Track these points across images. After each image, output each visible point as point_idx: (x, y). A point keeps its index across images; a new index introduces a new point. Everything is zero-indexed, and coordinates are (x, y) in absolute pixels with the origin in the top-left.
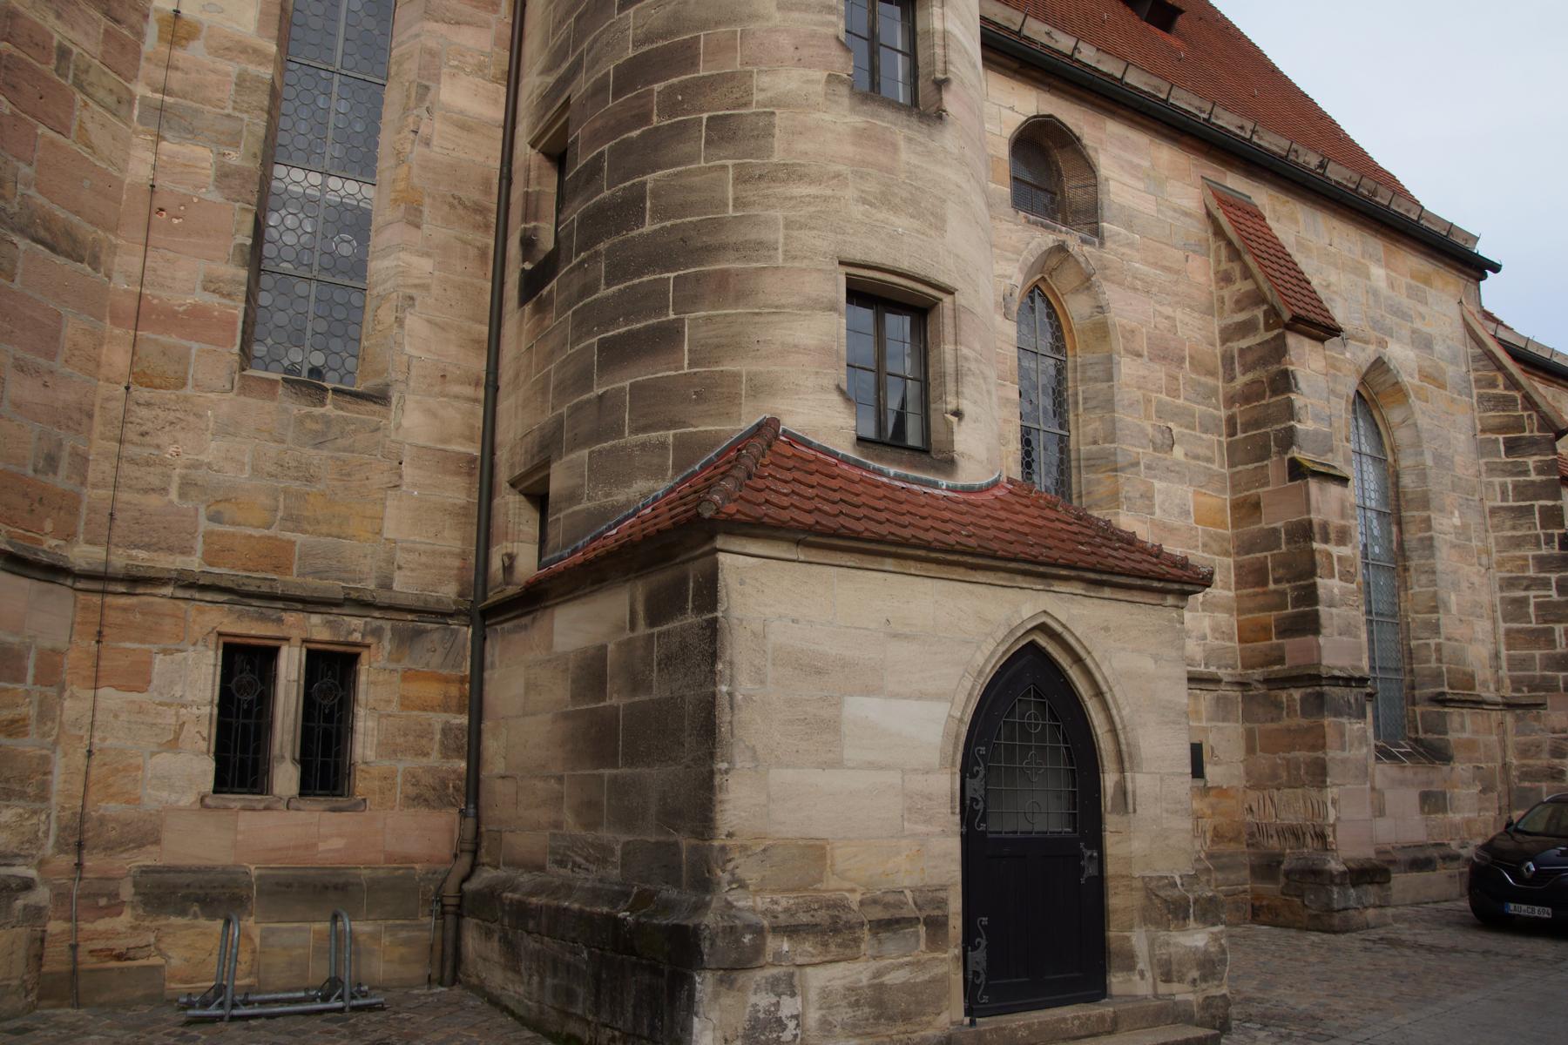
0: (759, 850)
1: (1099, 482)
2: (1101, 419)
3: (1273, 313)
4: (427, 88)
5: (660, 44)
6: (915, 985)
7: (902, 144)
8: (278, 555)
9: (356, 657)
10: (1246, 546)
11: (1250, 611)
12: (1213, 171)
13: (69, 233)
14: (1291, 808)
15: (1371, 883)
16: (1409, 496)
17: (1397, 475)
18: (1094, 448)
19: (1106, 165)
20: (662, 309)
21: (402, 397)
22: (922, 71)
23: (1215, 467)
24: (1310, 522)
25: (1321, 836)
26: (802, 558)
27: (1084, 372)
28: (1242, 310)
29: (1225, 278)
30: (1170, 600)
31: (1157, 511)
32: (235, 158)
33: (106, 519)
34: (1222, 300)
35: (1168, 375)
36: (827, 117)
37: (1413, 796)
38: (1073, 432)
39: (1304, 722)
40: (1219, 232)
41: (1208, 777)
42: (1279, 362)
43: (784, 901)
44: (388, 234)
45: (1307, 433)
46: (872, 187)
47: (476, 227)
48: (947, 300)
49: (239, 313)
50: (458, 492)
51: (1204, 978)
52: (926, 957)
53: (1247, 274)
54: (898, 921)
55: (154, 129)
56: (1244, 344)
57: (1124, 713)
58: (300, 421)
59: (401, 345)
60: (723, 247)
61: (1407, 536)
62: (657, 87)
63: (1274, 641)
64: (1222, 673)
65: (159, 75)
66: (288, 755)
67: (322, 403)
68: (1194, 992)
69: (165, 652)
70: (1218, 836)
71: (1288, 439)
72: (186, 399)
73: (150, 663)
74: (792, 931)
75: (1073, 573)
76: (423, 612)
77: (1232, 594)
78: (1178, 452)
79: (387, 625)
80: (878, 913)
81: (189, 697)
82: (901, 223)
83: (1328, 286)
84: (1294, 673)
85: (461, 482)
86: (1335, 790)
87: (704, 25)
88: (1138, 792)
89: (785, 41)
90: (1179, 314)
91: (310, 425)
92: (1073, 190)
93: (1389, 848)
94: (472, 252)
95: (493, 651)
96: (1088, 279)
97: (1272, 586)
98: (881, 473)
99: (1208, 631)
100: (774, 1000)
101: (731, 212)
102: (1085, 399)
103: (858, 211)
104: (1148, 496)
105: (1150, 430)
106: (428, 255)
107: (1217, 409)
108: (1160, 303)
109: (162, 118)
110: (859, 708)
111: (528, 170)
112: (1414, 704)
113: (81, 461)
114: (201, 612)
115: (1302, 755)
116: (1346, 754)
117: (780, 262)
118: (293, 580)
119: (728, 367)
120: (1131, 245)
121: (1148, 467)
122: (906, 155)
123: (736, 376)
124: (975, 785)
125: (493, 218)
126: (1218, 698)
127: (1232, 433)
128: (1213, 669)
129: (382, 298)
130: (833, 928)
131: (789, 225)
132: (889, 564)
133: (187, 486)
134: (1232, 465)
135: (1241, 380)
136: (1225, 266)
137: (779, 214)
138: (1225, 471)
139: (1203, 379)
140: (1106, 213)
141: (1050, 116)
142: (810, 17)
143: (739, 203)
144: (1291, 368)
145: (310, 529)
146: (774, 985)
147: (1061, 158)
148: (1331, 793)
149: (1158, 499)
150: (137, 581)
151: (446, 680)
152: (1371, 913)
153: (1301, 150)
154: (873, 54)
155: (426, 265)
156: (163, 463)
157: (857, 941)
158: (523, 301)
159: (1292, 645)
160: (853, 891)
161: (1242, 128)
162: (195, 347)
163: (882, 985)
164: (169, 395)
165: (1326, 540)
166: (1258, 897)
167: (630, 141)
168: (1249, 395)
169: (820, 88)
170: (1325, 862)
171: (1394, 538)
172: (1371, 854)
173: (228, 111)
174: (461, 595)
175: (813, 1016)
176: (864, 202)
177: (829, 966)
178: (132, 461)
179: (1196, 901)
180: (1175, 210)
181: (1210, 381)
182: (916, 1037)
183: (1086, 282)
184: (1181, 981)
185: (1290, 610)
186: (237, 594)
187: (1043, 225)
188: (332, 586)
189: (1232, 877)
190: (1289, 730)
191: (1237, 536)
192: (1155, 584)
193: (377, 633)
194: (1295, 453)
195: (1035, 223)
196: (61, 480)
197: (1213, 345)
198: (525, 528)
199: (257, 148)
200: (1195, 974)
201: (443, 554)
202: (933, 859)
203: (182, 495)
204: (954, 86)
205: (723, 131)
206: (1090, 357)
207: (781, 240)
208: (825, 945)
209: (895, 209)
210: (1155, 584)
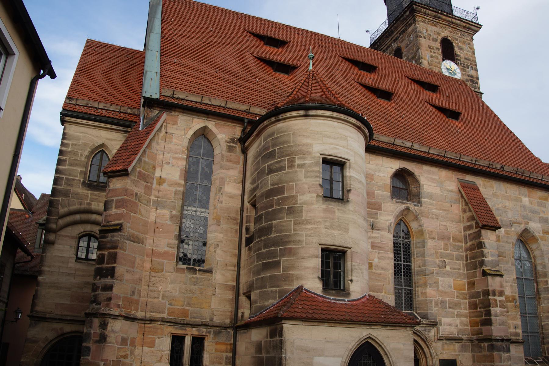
1: (421, 279)
3: (477, 223)
5: (276, 186)
7: (336, 211)
8: (185, 313)
9: (204, 338)
10: (472, 296)
11: (473, 317)
12: (461, 176)
13: (137, 238)
19: (423, 180)
20: (276, 257)
21: (216, 271)
22: (345, 187)
23: (461, 271)
24: (488, 290)
28: (469, 221)
29: (464, 211)
31: (440, 287)
32: (174, 212)
33: (145, 305)
34: (463, 218)
36: (316, 206)
39: (488, 353)
40: (462, 196)
42: (479, 239)
44: (212, 227)
45: (489, 261)
46: (328, 224)
47: (234, 224)
49: (176, 252)
50: (230, 295)
53: (470, 211)
55: (155, 207)
56: (470, 232)
58: (191, 279)
60: (290, 242)
62: (275, 198)
64: (464, 337)
65: (157, 193)
66: (187, 363)
67: (196, 274)
69: (158, 338)
71: (482, 263)
72: (163, 275)
73: (155, 341)
76: (221, 327)
77: (467, 311)
78: (448, 268)
79: (212, 330)
81: (164, 349)
82: (336, 232)
83: (505, 207)
85: (231, 292)
87: (286, 182)
89: (306, 186)
90: (448, 224)
91: (193, 280)
92: (413, 189)
94: (234, 231)
95: (239, 337)
97: (478, 310)
99: (458, 324)
101: (292, 232)
103: (324, 231)
104: (437, 283)
105: (438, 262)
106: (222, 233)
108: (442, 221)
109: (158, 204)
111: (247, 209)
113: (140, 291)
114: (167, 328)
116: (502, 364)
118: (189, 319)
120: (431, 204)
121: (437, 274)
122: (338, 214)
125: (239, 221)
126: (462, 345)
127: (467, 261)
128: (460, 336)
129: (211, 245)
131: (306, 236)
133: (164, 296)
134: (467, 271)
135: (469, 244)
136: (464, 207)
137: (304, 233)
138: (465, 272)
139: (457, 244)
140: (423, 195)
142: (312, 179)
143: (294, 230)
144: (483, 241)
147: (409, 179)
149: (440, 283)
150: (152, 320)
151: (227, 344)
153: (493, 164)
154: (331, 184)
155: (222, 236)
156: (158, 291)
158: (246, 246)
159: (484, 328)
161: (471, 160)
162: (165, 261)
164: (159, 274)
165: (494, 295)
167: (268, 212)
168: (471, 249)
169: (315, 199)
173: (173, 200)
174: (231, 322)
176: (326, 228)
178: (151, 291)
180: (447, 191)
181: (460, 244)
183: (416, 218)
185: (483, 318)
186: (175, 323)
188: (198, 321)
191: (469, 293)
193: (209, 332)
195: (399, 202)
196: (135, 297)
197: (461, 232)
198: (247, 305)
199: (179, 209)
201: (226, 312)
203: (162, 299)
204: (352, 191)
205: (291, 211)
206: (418, 240)
209: (334, 229)
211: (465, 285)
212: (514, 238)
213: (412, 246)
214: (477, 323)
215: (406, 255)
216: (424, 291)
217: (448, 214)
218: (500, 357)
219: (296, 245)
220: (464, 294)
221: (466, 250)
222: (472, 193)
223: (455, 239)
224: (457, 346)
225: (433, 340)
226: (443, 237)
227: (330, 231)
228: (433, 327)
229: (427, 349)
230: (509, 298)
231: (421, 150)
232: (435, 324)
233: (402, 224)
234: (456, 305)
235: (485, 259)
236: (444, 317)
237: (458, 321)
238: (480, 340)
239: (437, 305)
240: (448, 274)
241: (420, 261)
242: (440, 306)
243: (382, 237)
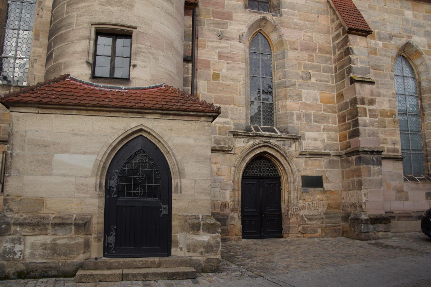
0: (18, 200)
1: (281, 92)
2: (281, 71)
3: (344, 29)
4: (41, 2)
6: (69, 244)
14: (350, 198)
15: (381, 223)
16: (424, 90)
17: (420, 83)
18: (279, 81)
23: (330, 84)
24: (356, 98)
25: (361, 207)
26: (40, 112)
27: (276, 57)
28: (337, 30)
29: (333, 21)
30: (203, 119)
31: (304, 100)
34: (332, 29)
35: (308, 55)
37: (423, 194)
38: (273, 77)
41: (325, 187)
43: (25, 216)
45: (357, 68)
48: (135, 31)
51: (207, 252)
52: (74, 236)
54: (63, 224)
56: (337, 41)
57: (177, 158)
59: (32, 72)
61: (424, 104)
63: (348, 140)
64: (332, 153)
68: (203, 257)
70: (329, 207)
71: (350, 70)
74: (21, 225)
75: (151, 111)
77: (337, 126)
78: (313, 80)
80: (58, 221)
82: (114, 9)
83: (384, 20)
84: (352, 151)
86: (366, 190)
88: (183, 186)
90: (314, 35)
93: (410, 212)
96: (275, 27)
98: (98, 86)
99: (326, 138)
100: (13, 245)
101: (65, 16)
102: (277, 66)
103: (98, 8)
104: (299, 95)
105: (301, 74)
108: (306, 32)
110: (59, 157)
112: (427, 162)
115: (356, 179)
116: (371, 178)
117: (74, 28)
119: (60, 61)
120: (294, 15)
121: (300, 85)
123: (61, 63)
124: (113, 183)
126: (330, 161)
128: (328, 151)
130: (39, 225)
132: (74, 112)
134: (336, 83)
135: (338, 53)
136: (332, 17)
139: (324, 55)
140: (283, 5)
143: (67, 13)
145: (6, 123)
146: (13, 241)
148: (363, 192)
149: (303, 96)
152: (380, 234)
155: (40, 50)
157: (46, 229)
159: (352, 140)
160: (53, 214)
163: (56, 244)
165: (363, 103)
166: (343, 228)
168: (339, 59)
170: (361, 215)
171: (419, 104)
172: (383, 213)
175: (28, 252)
176: (100, 4)
177: (36, 236)
179: (204, 224)
181: (328, 56)
182: (69, 261)
183: (275, 28)
184: (194, 252)
185: (351, 129)
187: (256, 12)
189: (334, 221)
190: (352, 170)
191: (338, 106)
192: (191, 113)
194: (352, 75)
195: (253, 12)
197: (329, 44)
200: (202, 250)
202: (92, 205)
206: (278, 52)
207: (75, 21)
208: (34, 229)
209: (111, 5)
210: (191, 113)
211: (333, 98)
212: (394, 52)
214: (346, 136)
216: (284, 104)
217: (314, 25)
218: (369, 171)
219: (67, 29)
220: (333, 107)
221: (335, 61)
223: (321, 50)
224: (324, 161)
225: (294, 155)
227: (106, 8)
228: (295, 142)
229: (288, 165)
230: (387, 112)
232: (296, 139)
233: (260, 37)
234: (324, 119)
235: (353, 66)
236: (308, 131)
237: (325, 135)
238: (349, 154)
239: (299, 118)
240: (313, 87)
241: (280, 73)
242: (303, 119)
243: (232, 47)
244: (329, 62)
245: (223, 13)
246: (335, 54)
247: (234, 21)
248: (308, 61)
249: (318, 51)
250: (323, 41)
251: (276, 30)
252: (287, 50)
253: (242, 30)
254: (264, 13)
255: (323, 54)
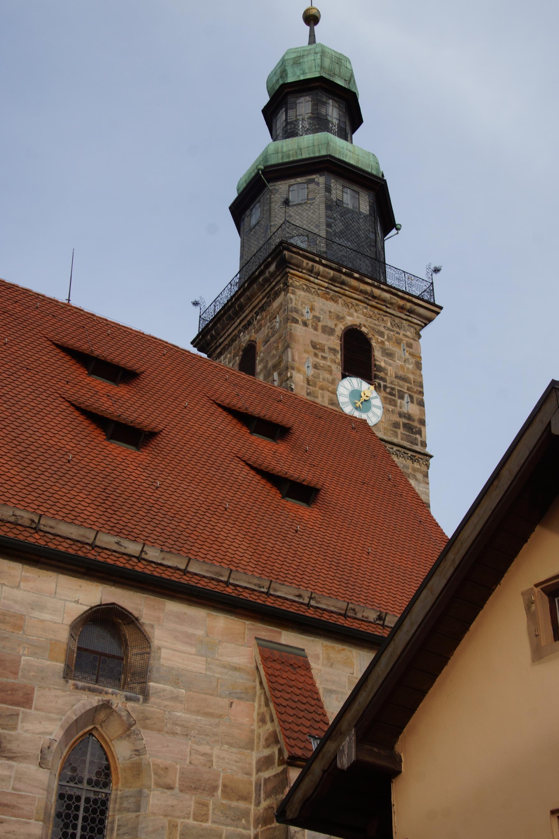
12: (267, 632)
19: (160, 637)
27: (121, 803)
29: (262, 720)
90: (216, 751)
92: (134, 658)
107: (246, 828)
108: (198, 743)
120: (175, 698)
135: (264, 804)
136: (264, 709)
139: (234, 804)
140: (154, 674)
141: (113, 604)
147: (127, 631)
153: (357, 609)
161: (300, 596)
180: (224, 667)
181: (242, 805)
187: (90, 690)
195: (83, 689)
197: (249, 774)
213: (111, 805)
215: (92, 830)
222: (285, 675)
223: (229, 791)
226: (196, 785)
231: (165, 563)
243: (19, 778)
244: (244, 821)
245: (12, 690)
246: (258, 804)
247: (36, 709)
248: (195, 819)
249: (220, 791)
250: (234, 768)
251: (129, 736)
252: (149, 788)
253: (50, 734)
254: (107, 693)
255: (230, 799)
